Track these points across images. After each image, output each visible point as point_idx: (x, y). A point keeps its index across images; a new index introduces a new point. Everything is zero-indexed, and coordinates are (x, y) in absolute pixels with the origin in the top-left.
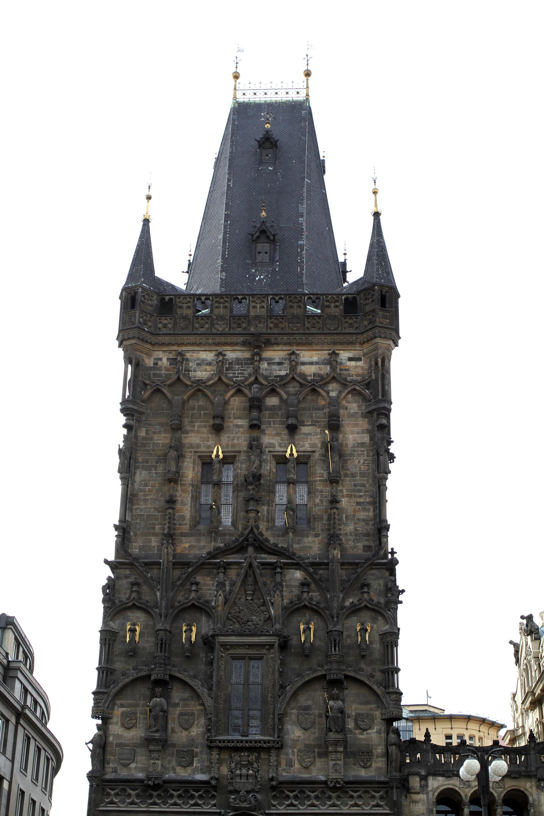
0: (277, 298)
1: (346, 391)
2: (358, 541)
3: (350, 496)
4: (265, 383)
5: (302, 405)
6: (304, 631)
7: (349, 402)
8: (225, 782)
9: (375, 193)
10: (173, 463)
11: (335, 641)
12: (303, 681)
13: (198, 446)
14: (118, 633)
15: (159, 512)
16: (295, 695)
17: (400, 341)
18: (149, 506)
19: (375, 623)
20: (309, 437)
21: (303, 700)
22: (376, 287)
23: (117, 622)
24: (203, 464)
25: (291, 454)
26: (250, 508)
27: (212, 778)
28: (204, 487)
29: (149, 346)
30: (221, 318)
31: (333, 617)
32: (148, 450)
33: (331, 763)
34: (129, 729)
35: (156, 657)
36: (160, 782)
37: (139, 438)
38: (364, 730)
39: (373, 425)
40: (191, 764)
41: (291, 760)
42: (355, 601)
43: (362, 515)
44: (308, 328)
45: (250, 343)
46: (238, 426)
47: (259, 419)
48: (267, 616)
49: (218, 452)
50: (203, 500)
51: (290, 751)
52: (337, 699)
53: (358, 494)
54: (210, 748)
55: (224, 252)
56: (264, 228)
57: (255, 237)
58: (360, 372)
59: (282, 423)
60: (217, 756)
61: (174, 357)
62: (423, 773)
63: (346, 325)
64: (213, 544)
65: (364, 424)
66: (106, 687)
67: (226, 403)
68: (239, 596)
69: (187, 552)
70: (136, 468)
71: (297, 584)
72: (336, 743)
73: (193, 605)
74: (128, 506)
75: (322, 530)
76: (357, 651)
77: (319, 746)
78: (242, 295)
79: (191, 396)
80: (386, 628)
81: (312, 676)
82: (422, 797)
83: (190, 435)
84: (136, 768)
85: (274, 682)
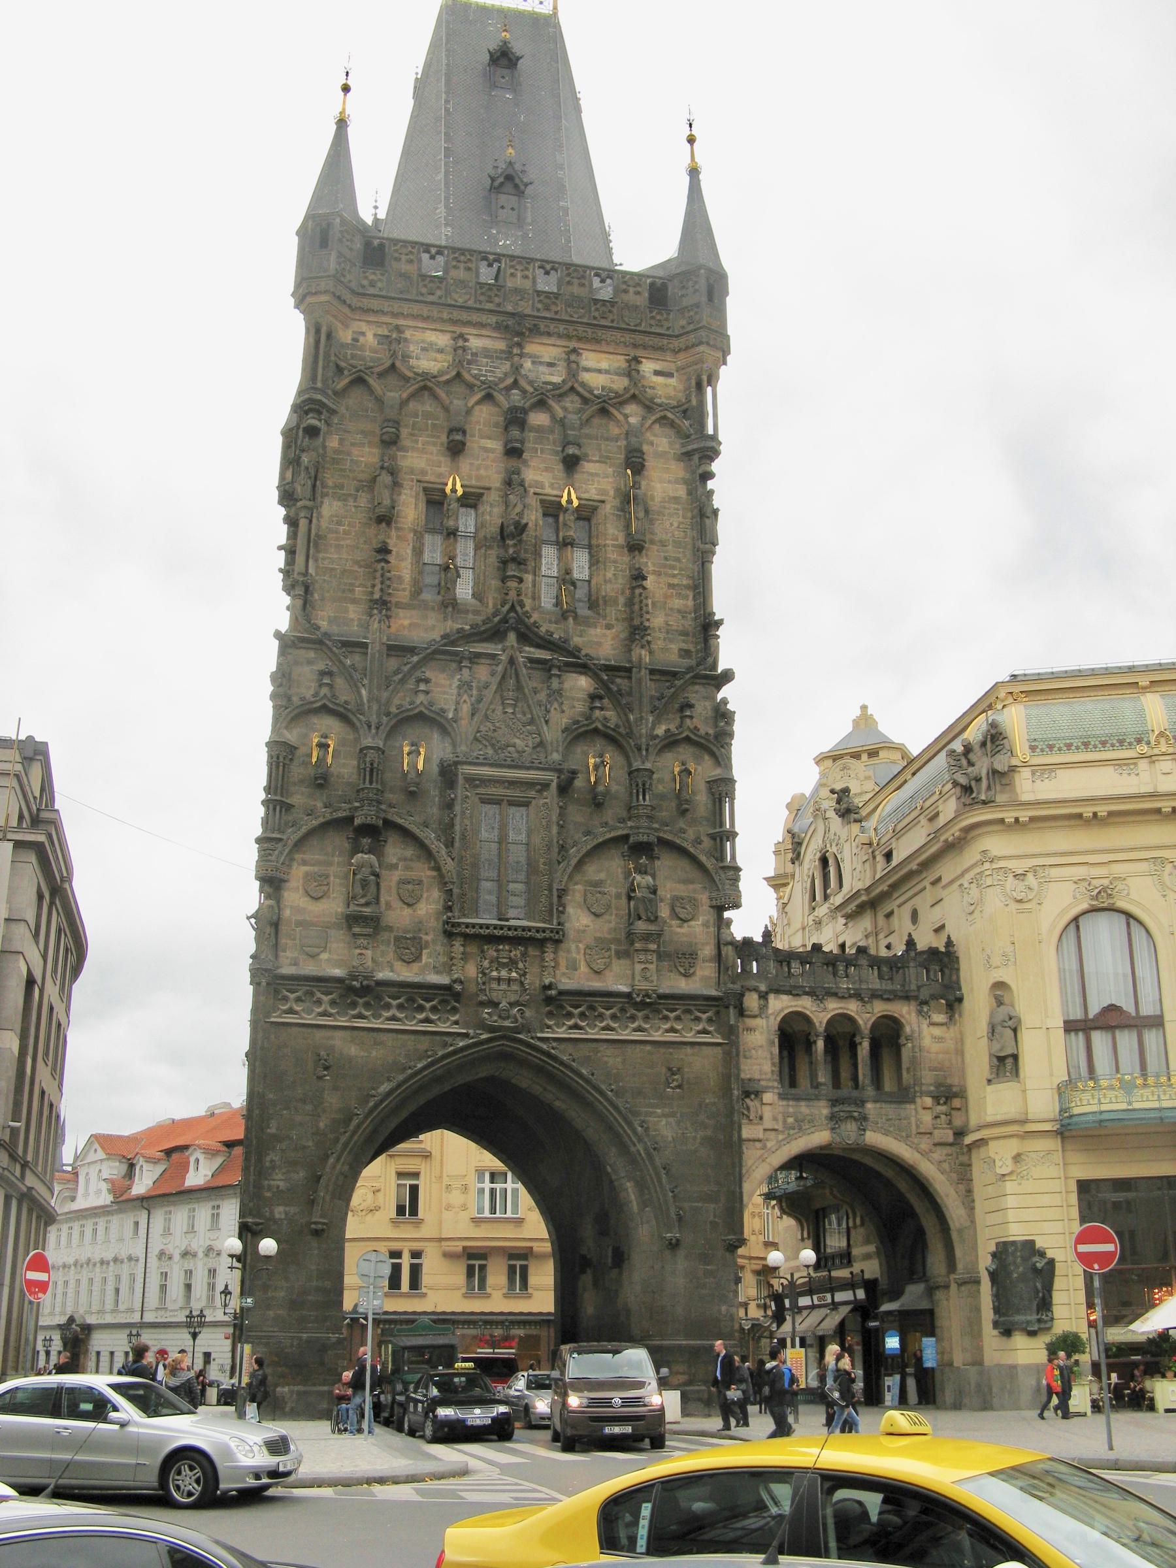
0: (548, 267)
1: (653, 418)
2: (671, 641)
3: (659, 574)
4: (531, 390)
5: (586, 431)
6: (596, 767)
7: (655, 435)
8: (473, 988)
9: (691, 140)
10: (386, 493)
11: (644, 785)
12: (596, 842)
13: (423, 472)
14: (296, 748)
15: (361, 567)
16: (580, 863)
17: (729, 358)
18: (344, 556)
19: (699, 764)
20: (596, 479)
21: (593, 871)
22: (702, 271)
23: (296, 732)
24: (429, 502)
25: (570, 501)
26: (509, 573)
27: (455, 981)
28: (428, 538)
29: (347, 310)
30: (462, 283)
31: (639, 749)
32: (341, 470)
33: (638, 967)
34: (317, 899)
35: (363, 789)
36: (373, 984)
37: (328, 450)
38: (684, 921)
39: (693, 472)
40: (418, 958)
41: (575, 961)
42: (672, 727)
43: (677, 603)
44: (595, 318)
45: (507, 327)
46: (486, 450)
47: (522, 442)
48: (538, 740)
49: (455, 485)
50: (427, 558)
51: (573, 947)
52: (646, 873)
53: (670, 572)
54: (449, 935)
55: (447, 199)
56: (510, 171)
57: (496, 184)
58: (672, 393)
59: (557, 453)
60: (462, 949)
61: (386, 333)
62: (763, 988)
63: (653, 322)
64: (449, 623)
65: (678, 470)
66: (280, 831)
67: (469, 412)
68: (492, 707)
69: (406, 632)
70: (324, 495)
71: (582, 695)
72: (647, 937)
73: (421, 712)
74: (311, 552)
75: (617, 619)
76: (673, 804)
77: (616, 941)
78: (495, 254)
79: (413, 396)
80: (717, 772)
81: (608, 836)
82: (759, 1022)
83: (409, 454)
84: (328, 960)
85: (551, 842)
